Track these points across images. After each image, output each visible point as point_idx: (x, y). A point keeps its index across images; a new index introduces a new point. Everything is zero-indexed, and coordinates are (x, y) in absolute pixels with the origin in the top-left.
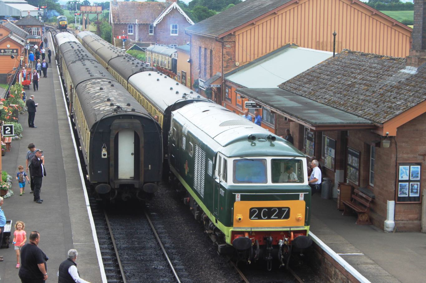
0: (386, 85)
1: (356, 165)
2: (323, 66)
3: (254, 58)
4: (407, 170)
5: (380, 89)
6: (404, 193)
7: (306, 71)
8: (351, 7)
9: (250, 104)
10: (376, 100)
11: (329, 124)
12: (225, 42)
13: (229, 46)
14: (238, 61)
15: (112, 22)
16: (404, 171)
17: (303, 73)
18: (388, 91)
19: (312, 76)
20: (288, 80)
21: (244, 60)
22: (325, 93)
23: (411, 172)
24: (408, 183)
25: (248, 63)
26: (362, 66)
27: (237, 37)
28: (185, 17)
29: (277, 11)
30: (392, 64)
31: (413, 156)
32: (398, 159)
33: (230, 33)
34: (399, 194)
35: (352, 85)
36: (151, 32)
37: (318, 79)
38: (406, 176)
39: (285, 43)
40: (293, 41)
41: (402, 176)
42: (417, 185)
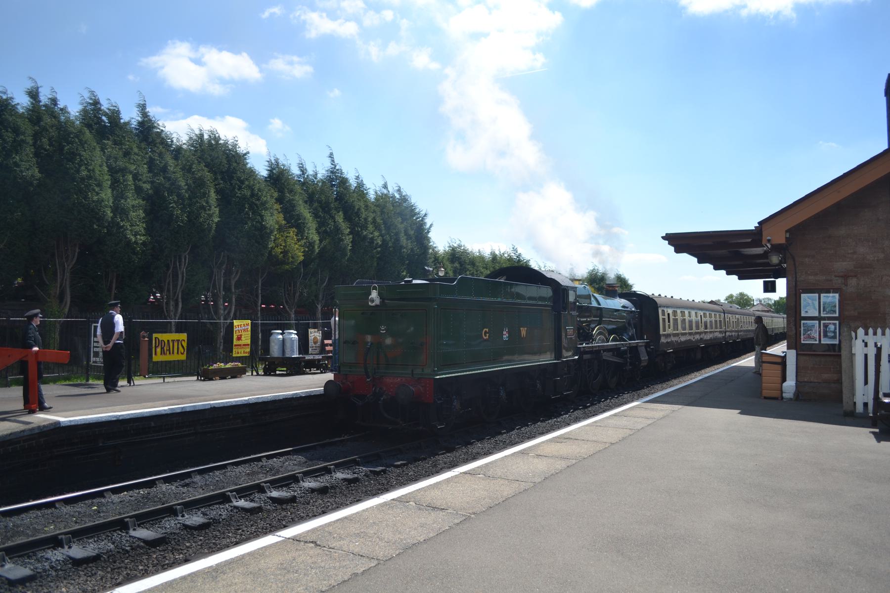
4: (816, 300)
6: (812, 337)
16: (810, 301)
23: (822, 303)
24: (817, 322)
31: (824, 278)
34: (802, 340)
41: (806, 310)
42: (835, 324)
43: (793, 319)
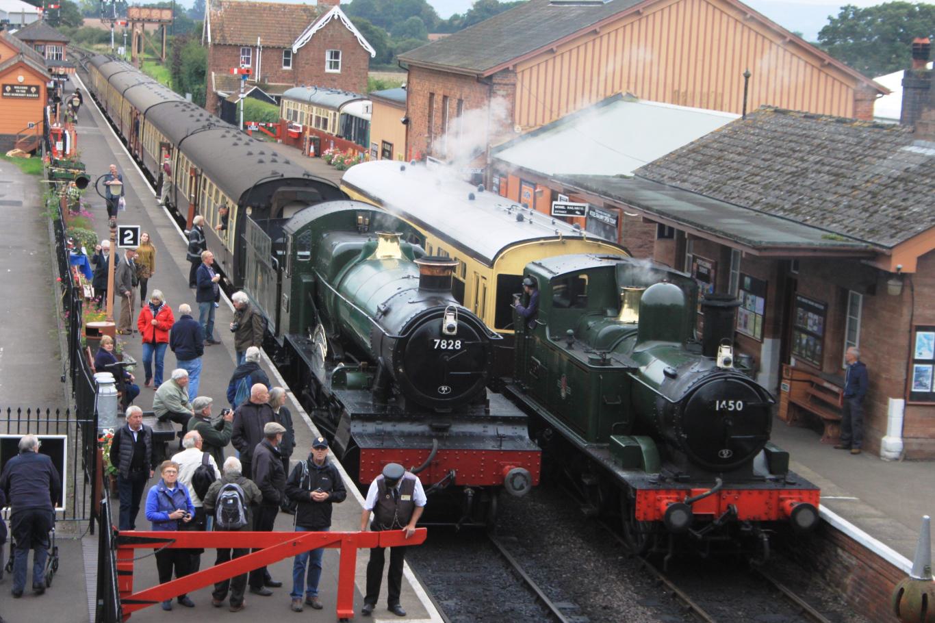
0: (878, 175)
1: (815, 328)
2: (725, 136)
3: (551, 118)
5: (867, 181)
7: (687, 146)
8: (743, 25)
9: (563, 207)
10: (863, 202)
11: (784, 246)
14: (520, 124)
15: (209, 40)
17: (682, 148)
18: (886, 186)
19: (704, 155)
20: (650, 161)
21: (532, 122)
22: (744, 187)
25: (538, 127)
26: (814, 138)
27: (519, 76)
28: (356, 37)
29: (600, 28)
30: (880, 135)
32: (914, 318)
33: (506, 67)
35: (803, 173)
36: (287, 63)
37: (720, 161)
39: (612, 92)
40: (628, 88)
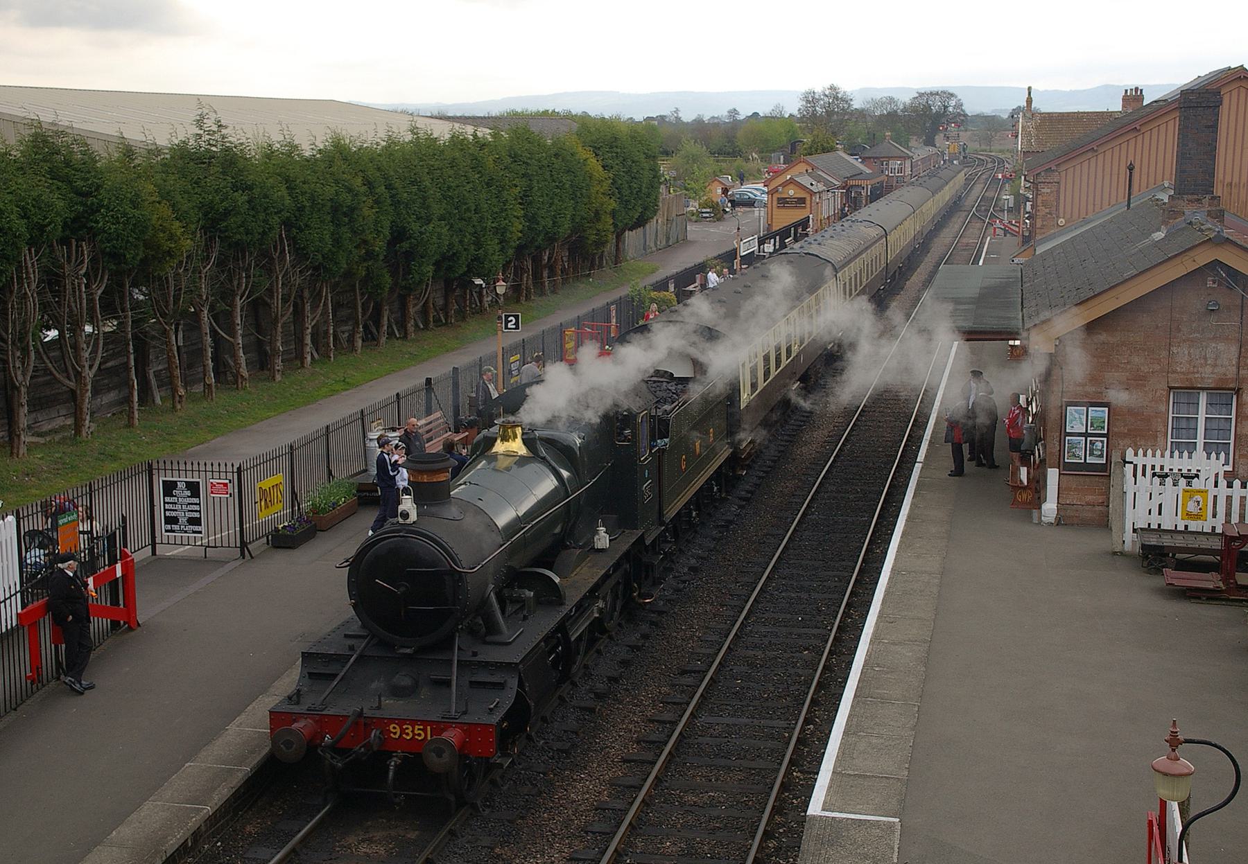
12: (1040, 183)
13: (1049, 191)
23: (1089, 418)
24: (1084, 438)
34: (1066, 457)
38: (1080, 425)
41: (1072, 425)
42: (1102, 442)
43: (1058, 434)
